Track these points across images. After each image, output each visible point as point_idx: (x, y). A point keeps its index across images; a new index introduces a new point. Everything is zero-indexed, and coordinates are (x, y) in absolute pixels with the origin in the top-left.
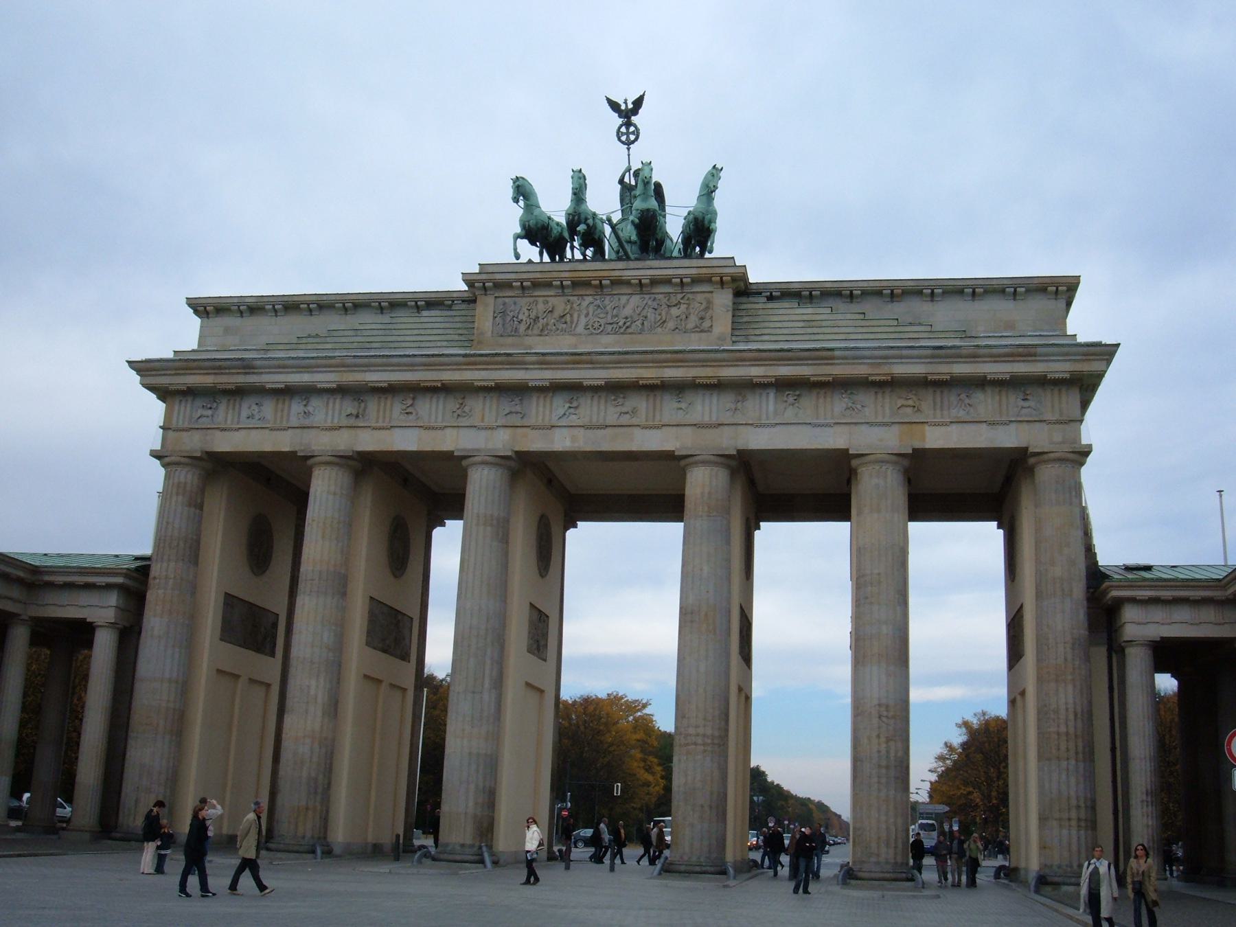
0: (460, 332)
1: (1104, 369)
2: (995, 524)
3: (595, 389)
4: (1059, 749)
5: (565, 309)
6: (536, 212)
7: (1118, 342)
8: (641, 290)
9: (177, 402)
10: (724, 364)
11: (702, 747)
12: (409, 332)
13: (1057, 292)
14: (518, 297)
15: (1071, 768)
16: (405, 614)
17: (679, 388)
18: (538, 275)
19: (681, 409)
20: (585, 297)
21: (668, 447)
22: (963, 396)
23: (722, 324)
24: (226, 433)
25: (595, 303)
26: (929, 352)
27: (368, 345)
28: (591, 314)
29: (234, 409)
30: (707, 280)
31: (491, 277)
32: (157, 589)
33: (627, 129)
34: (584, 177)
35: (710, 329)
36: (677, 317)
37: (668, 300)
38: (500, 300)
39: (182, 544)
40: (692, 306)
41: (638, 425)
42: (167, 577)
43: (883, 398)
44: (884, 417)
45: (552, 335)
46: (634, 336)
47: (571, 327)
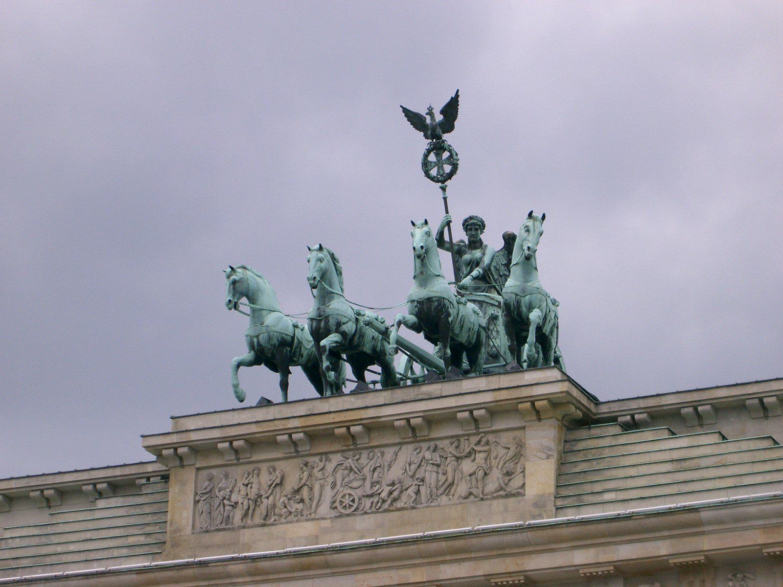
0: (148, 529)
5: (301, 479)
6: (270, 319)
8: (415, 436)
10: (531, 549)
14: (231, 465)
18: (254, 429)
20: (331, 456)
27: (14, 564)
31: (184, 438)
33: (438, 155)
34: (332, 256)
35: (521, 491)
36: (470, 475)
37: (457, 447)
38: (204, 473)
40: (493, 454)
45: (282, 524)
46: (406, 511)
47: (311, 506)
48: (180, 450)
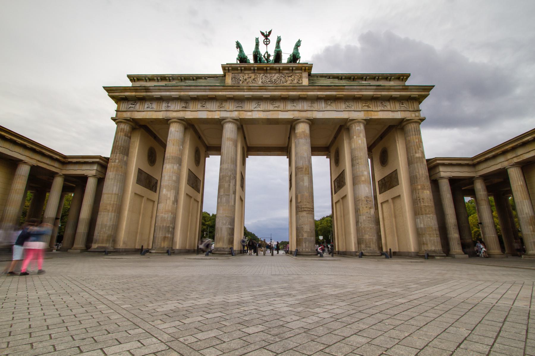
4: (426, 211)
9: (122, 103)
11: (308, 212)
13: (402, 79)
15: (431, 217)
16: (198, 178)
19: (293, 106)
23: (305, 82)
24: (139, 113)
26: (375, 87)
29: (142, 105)
30: (301, 69)
31: (231, 66)
33: (267, 40)
38: (233, 74)
39: (122, 148)
41: (280, 111)
42: (115, 159)
43: (358, 103)
44: (359, 109)
48: (230, 68)
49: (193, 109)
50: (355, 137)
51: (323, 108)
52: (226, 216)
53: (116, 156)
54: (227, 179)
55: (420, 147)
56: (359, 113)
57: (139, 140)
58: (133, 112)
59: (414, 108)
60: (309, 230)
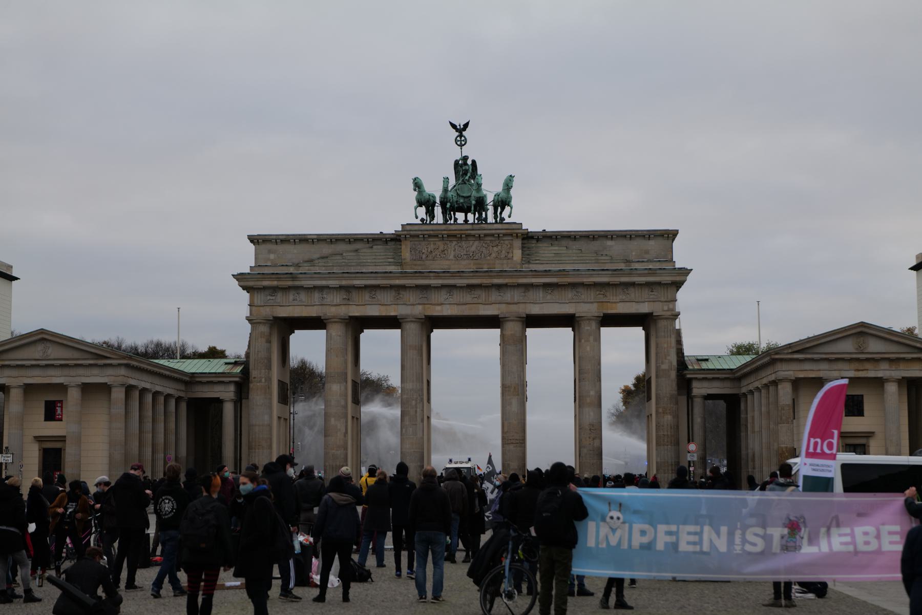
1: (684, 279)
2: (641, 328)
3: (461, 287)
6: (424, 194)
7: (692, 268)
9: (256, 293)
11: (515, 445)
12: (368, 258)
17: (499, 287)
18: (431, 232)
19: (500, 295)
21: (495, 312)
22: (625, 290)
23: (517, 254)
25: (459, 245)
26: (610, 272)
27: (349, 264)
28: (457, 249)
30: (511, 235)
31: (409, 232)
32: (257, 383)
33: (461, 138)
38: (412, 242)
39: (266, 361)
44: (591, 299)
49: (359, 302)
50: (583, 341)
51: (541, 299)
52: (414, 451)
53: (260, 374)
54: (414, 403)
55: (669, 355)
56: (590, 304)
57: (276, 339)
58: (274, 307)
59: (667, 298)
60: (517, 467)
